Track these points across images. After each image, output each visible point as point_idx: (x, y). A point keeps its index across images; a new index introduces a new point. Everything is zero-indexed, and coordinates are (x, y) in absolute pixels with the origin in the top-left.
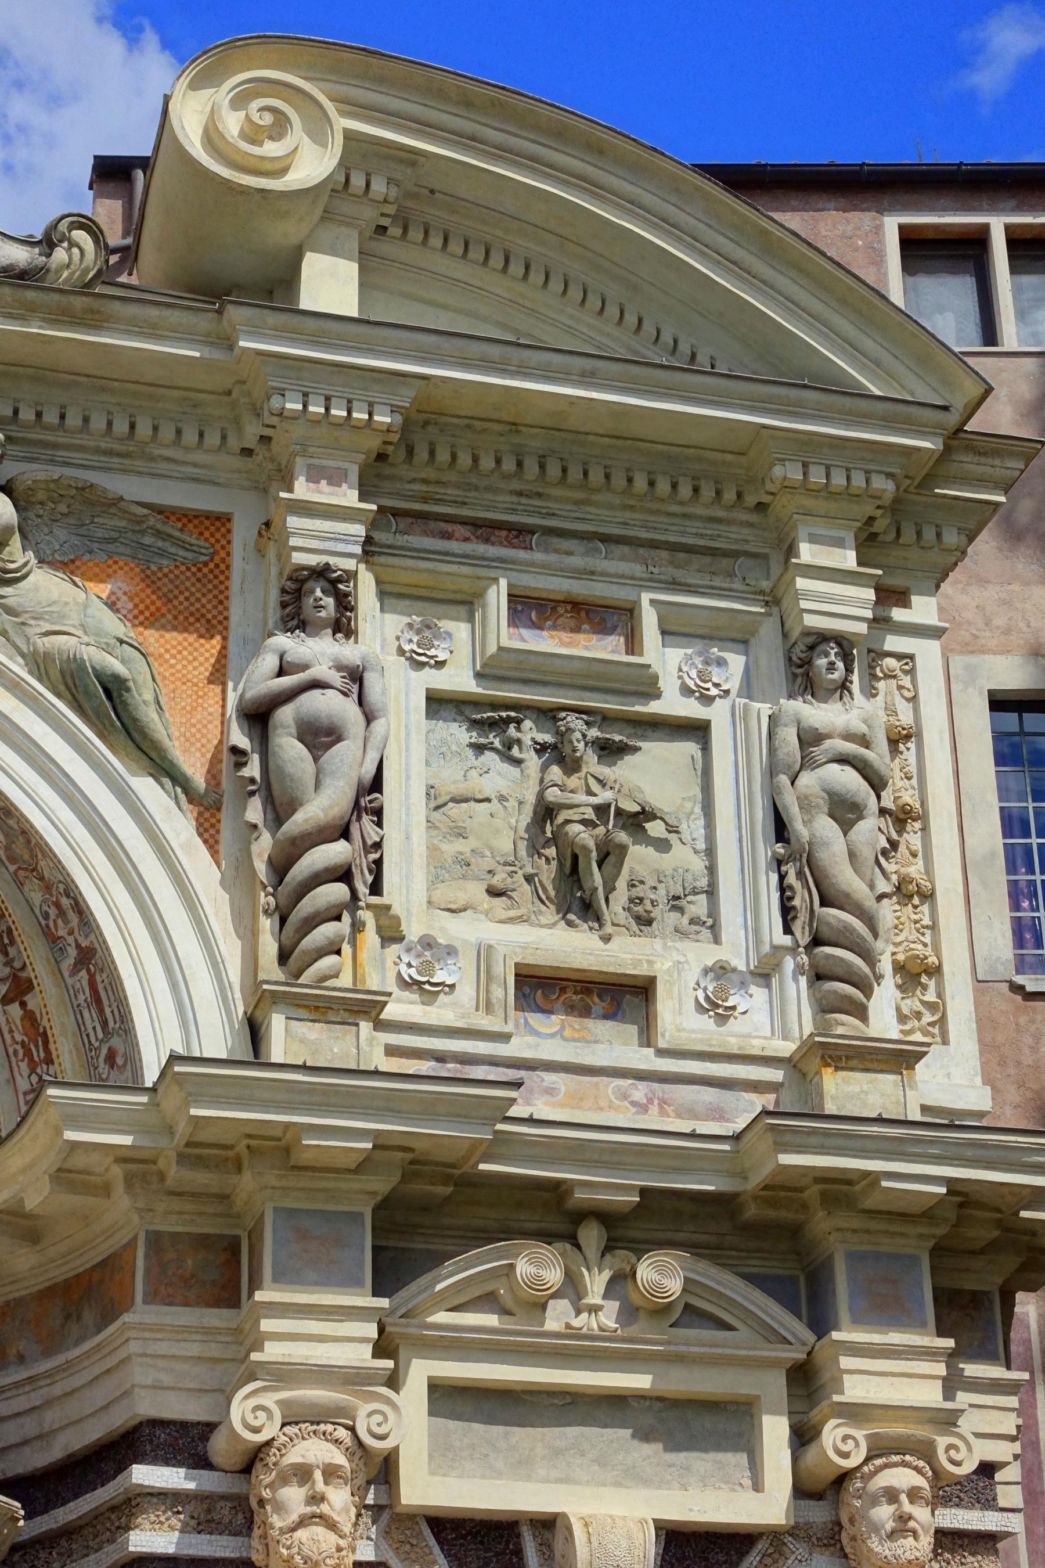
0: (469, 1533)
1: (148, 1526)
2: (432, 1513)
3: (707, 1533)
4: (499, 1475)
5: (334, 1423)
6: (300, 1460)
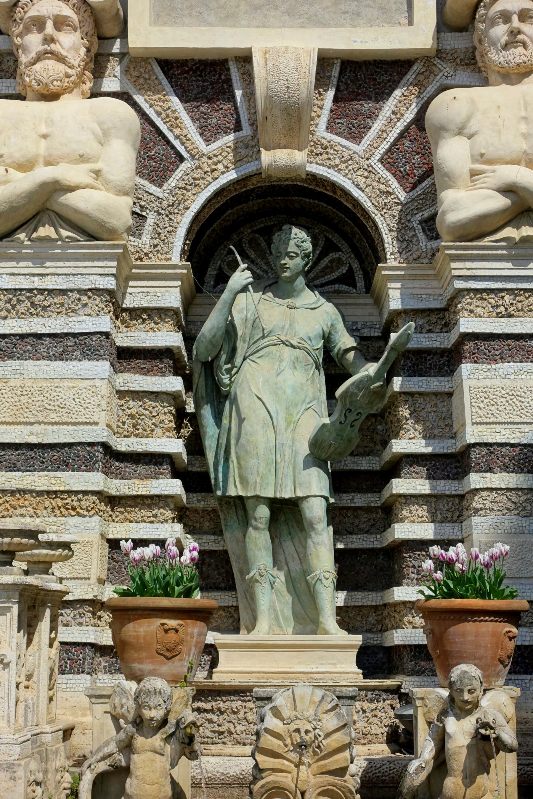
0: (191, 69)
4: (211, 25)
6: (36, 14)
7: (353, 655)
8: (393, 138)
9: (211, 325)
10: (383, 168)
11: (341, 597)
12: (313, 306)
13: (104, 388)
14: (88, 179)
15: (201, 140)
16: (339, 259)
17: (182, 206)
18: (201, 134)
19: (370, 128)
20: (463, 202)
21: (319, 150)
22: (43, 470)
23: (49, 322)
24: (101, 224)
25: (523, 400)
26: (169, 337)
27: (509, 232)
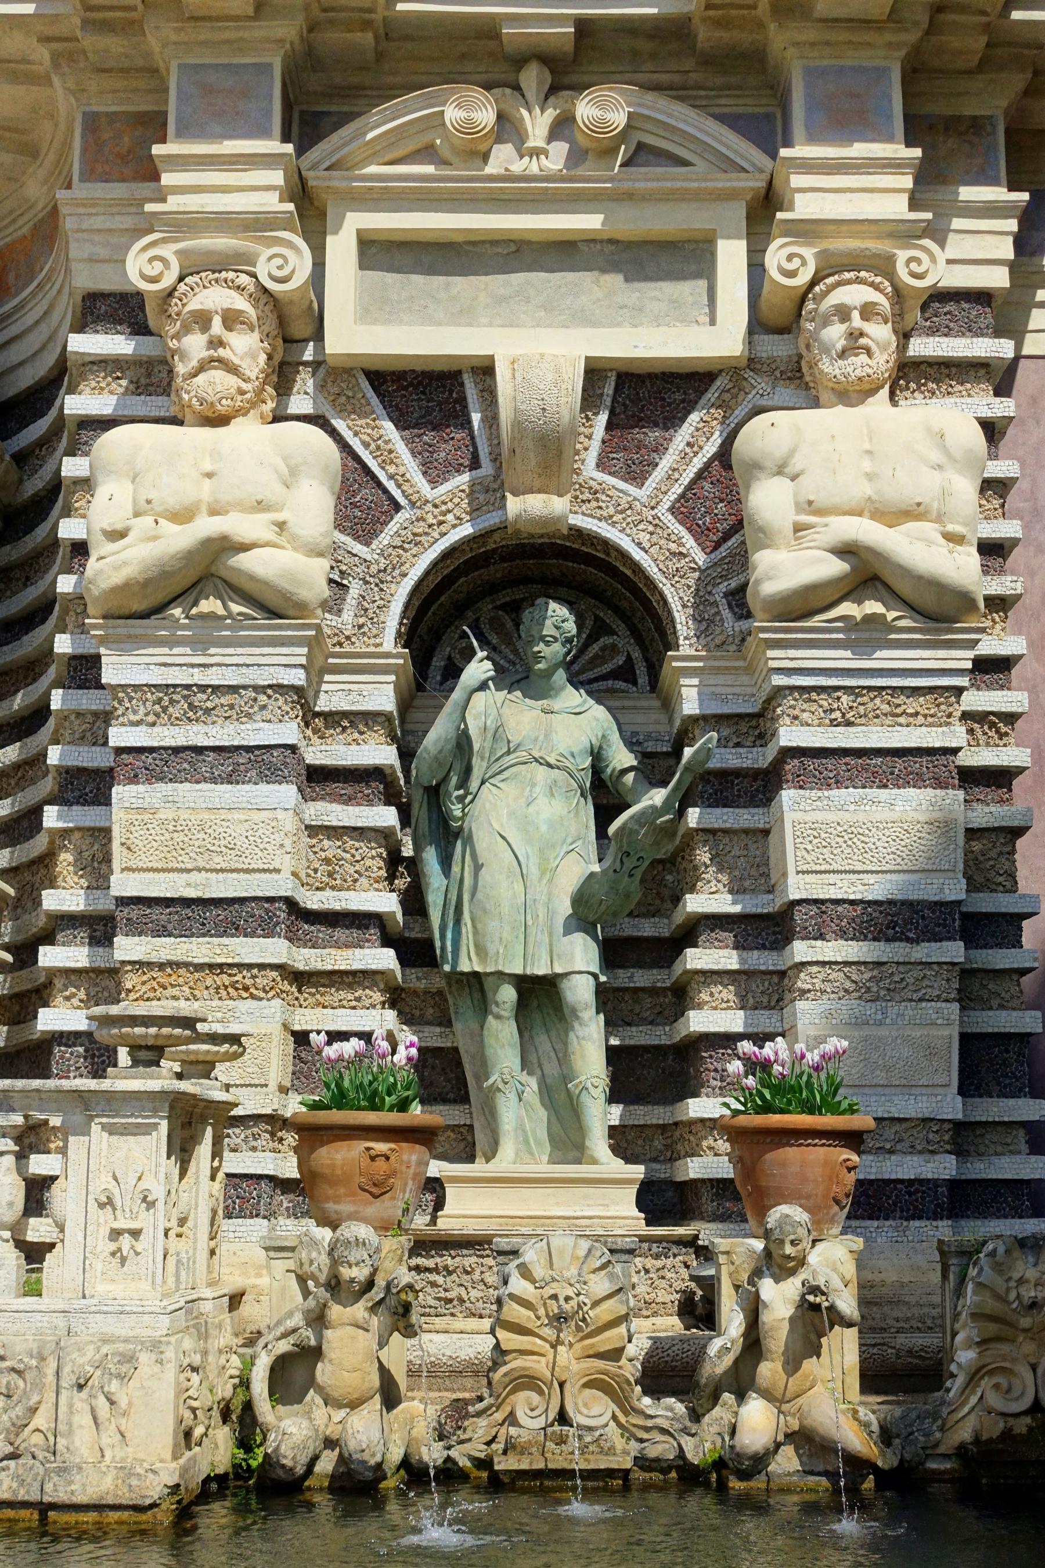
0: (411, 384)
1: (88, 390)
2: (373, 367)
3: (664, 373)
5: (236, 271)
6: (199, 307)
7: (632, 1192)
8: (688, 480)
9: (437, 735)
10: (673, 521)
11: (615, 1113)
12: (577, 710)
13: (289, 822)
14: (268, 534)
15: (424, 481)
16: (614, 646)
17: (397, 572)
18: (424, 473)
19: (657, 465)
20: (784, 567)
21: (587, 496)
22: (204, 935)
23: (213, 730)
24: (286, 596)
25: (867, 840)
26: (378, 752)
27: (848, 608)
